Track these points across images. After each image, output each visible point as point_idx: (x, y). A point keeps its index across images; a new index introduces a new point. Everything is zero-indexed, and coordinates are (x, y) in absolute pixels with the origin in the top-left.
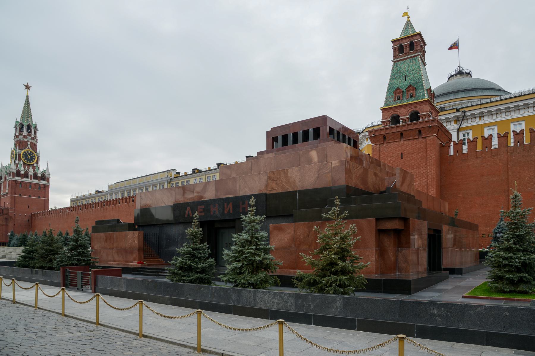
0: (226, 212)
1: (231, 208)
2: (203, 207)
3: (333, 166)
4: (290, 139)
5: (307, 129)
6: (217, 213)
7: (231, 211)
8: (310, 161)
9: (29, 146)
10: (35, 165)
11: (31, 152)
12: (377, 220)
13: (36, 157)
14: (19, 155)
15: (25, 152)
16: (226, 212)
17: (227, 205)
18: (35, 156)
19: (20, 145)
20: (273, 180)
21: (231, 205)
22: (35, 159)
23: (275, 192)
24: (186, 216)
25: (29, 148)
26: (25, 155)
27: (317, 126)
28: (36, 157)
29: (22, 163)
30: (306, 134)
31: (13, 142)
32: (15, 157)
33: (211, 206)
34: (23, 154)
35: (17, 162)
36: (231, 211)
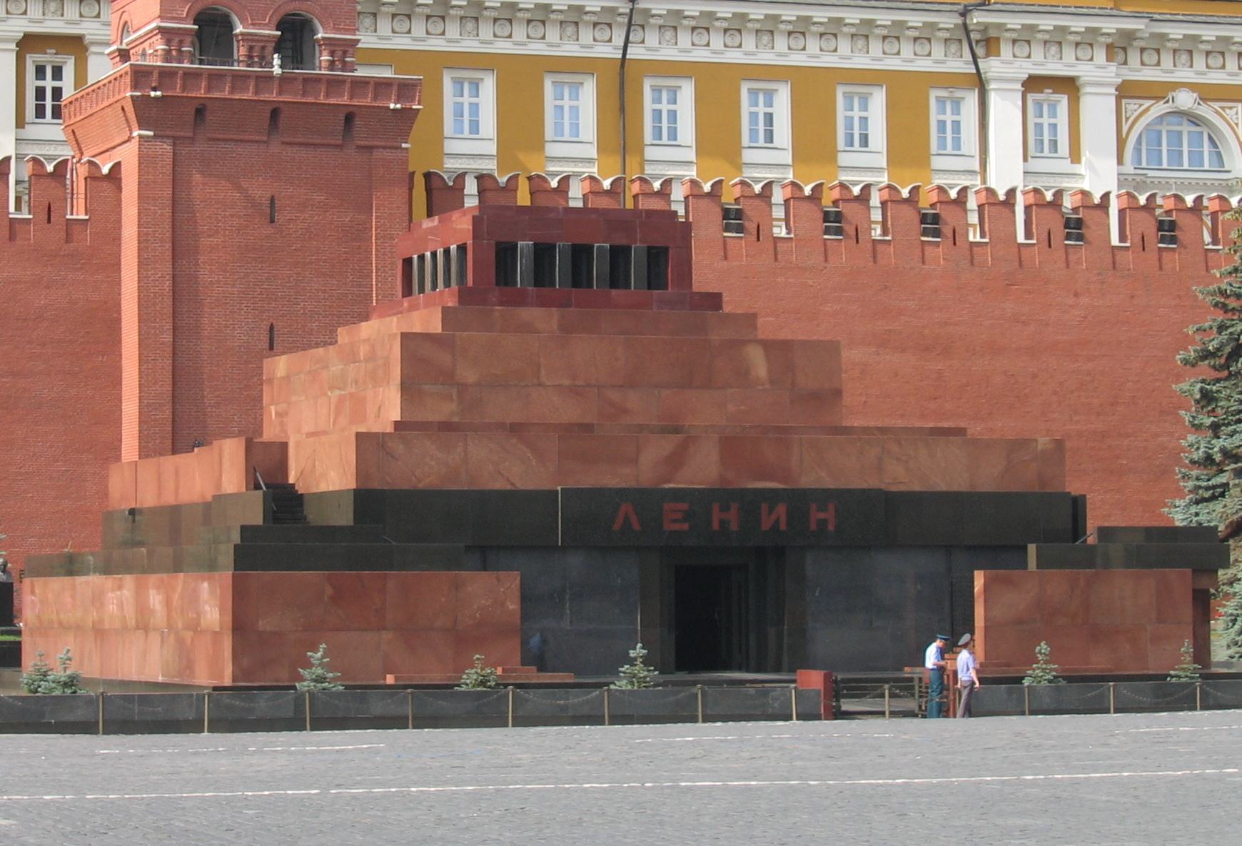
0: (766, 524)
1: (783, 519)
2: (685, 506)
3: (1039, 447)
4: (597, 268)
5: (623, 242)
6: (734, 527)
7: (783, 527)
8: (743, 374)
12: (1194, 571)
16: (766, 524)
17: (771, 510)
20: (898, 459)
21: (781, 509)
23: (903, 488)
24: (616, 527)
27: (660, 243)
30: (619, 255)
33: (716, 507)
36: (783, 527)
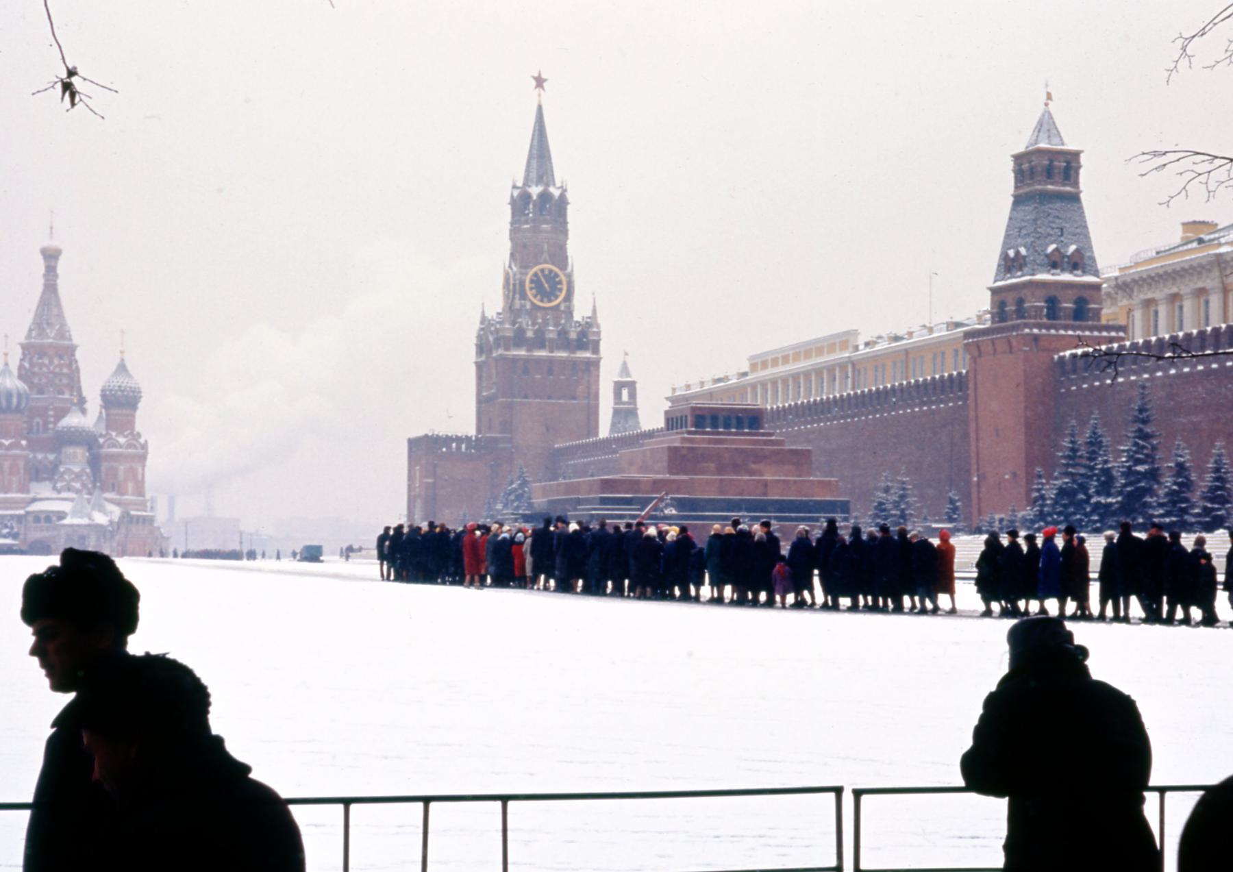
9: (545, 255)
10: (562, 307)
11: (551, 271)
13: (565, 282)
14: (522, 284)
15: (536, 275)
18: (560, 282)
19: (522, 252)
22: (561, 290)
25: (546, 262)
26: (536, 281)
28: (565, 282)
29: (528, 306)
31: (505, 246)
32: (514, 289)
34: (532, 281)
35: (517, 303)
